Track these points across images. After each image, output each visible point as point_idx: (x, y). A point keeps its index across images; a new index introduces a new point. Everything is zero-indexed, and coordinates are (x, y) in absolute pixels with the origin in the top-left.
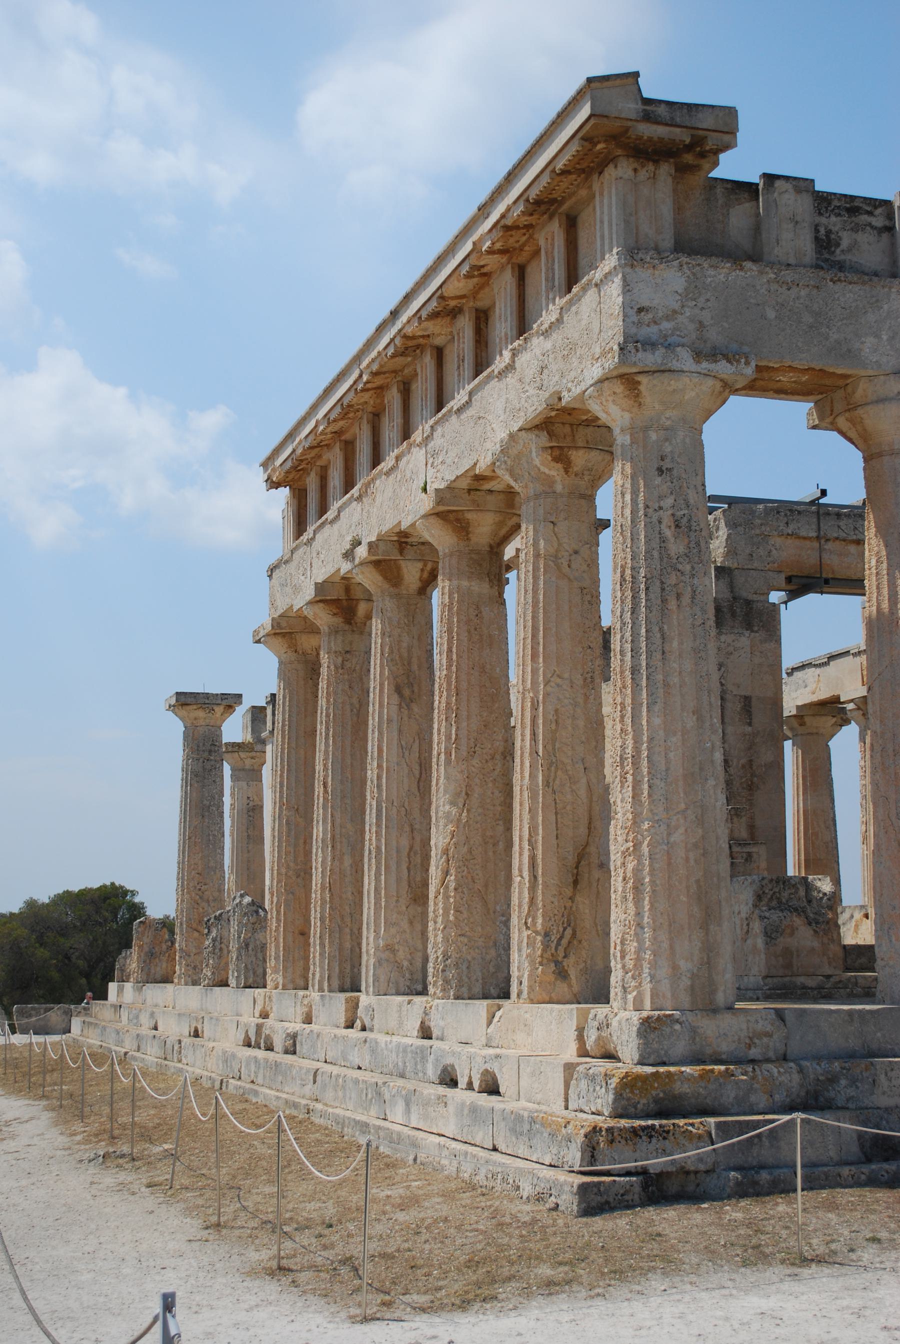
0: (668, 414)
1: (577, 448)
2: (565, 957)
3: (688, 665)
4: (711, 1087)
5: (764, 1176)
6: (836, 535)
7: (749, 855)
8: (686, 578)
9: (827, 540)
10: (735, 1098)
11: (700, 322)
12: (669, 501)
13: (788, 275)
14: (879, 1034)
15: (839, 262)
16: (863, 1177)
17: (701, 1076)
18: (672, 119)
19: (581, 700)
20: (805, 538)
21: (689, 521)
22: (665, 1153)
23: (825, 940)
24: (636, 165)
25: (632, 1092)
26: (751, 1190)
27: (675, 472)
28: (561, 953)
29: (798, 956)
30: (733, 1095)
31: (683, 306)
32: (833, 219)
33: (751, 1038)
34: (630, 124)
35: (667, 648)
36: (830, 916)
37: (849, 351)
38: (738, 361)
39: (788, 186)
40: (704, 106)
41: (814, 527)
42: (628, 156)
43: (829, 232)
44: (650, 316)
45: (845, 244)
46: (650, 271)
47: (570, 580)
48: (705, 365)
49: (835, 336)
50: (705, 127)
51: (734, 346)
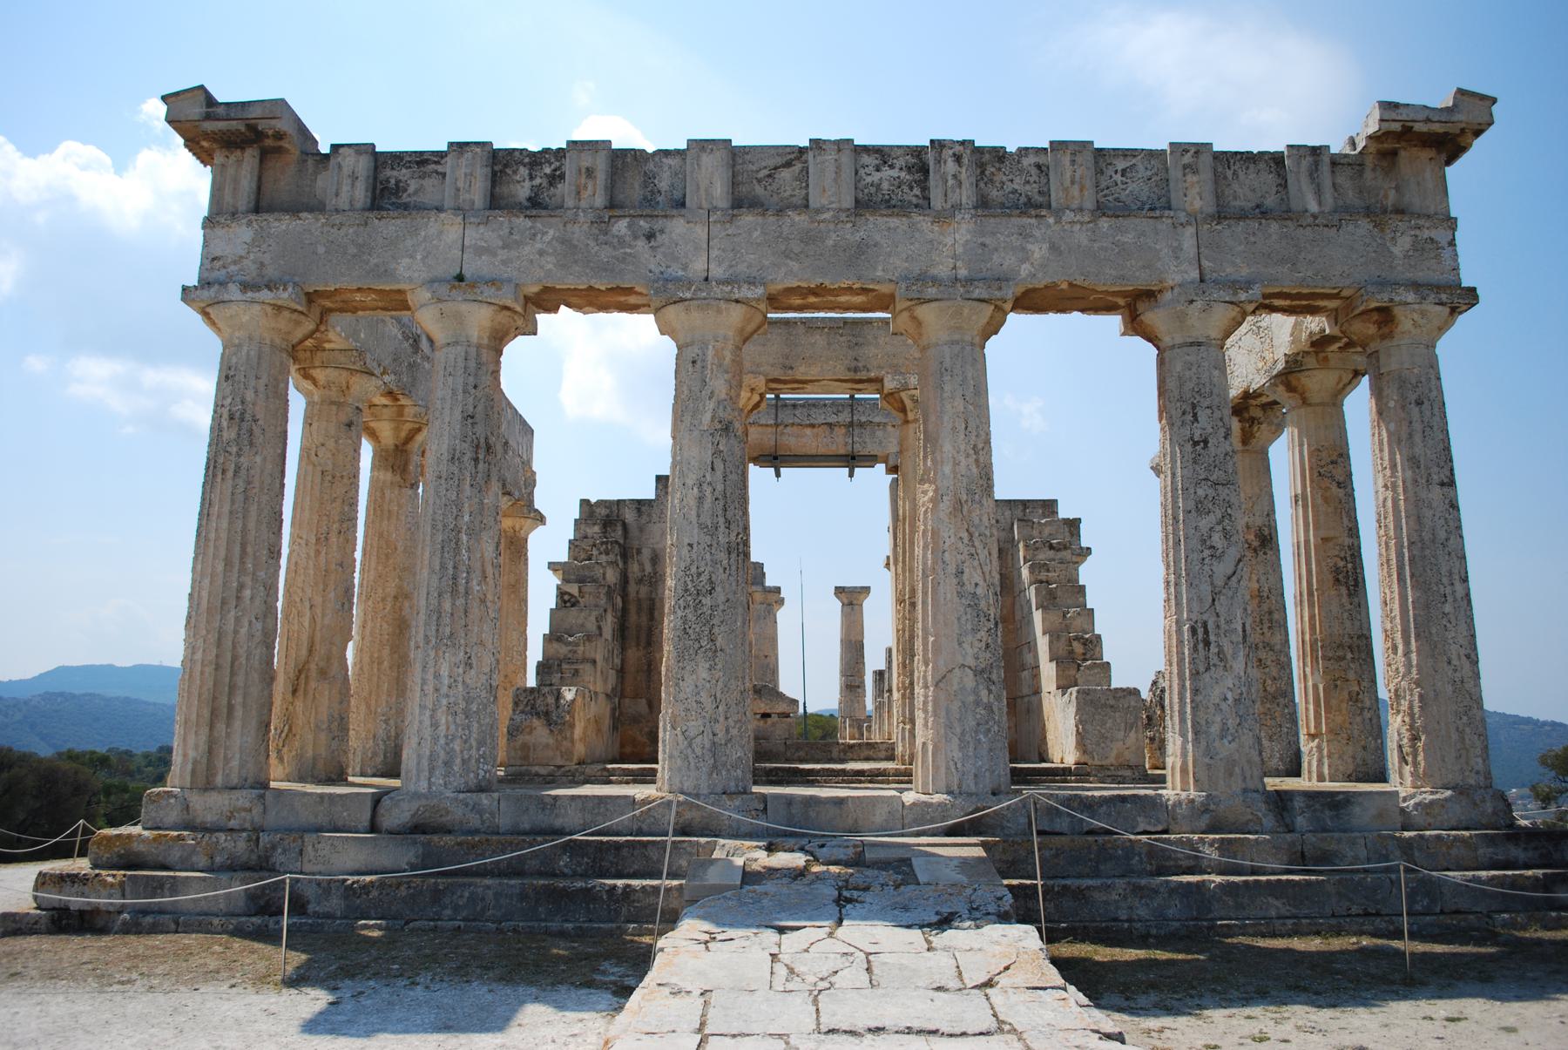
0: (237, 334)
1: (315, 367)
2: (283, 746)
3: (225, 524)
4: (161, 847)
5: (149, 919)
6: (791, 421)
7: (577, 671)
8: (232, 458)
9: (786, 426)
10: (181, 857)
11: (262, 264)
12: (229, 400)
13: (337, 219)
14: (345, 814)
15: (405, 204)
16: (231, 927)
17: (155, 839)
18: (227, 115)
19: (312, 554)
20: (767, 426)
21: (242, 414)
22: (83, 895)
23: (559, 738)
24: (227, 153)
25: (98, 848)
26: (134, 929)
27: (236, 378)
28: (281, 744)
29: (534, 750)
30: (178, 855)
31: (248, 253)
32: (404, 171)
33: (232, 813)
34: (197, 123)
35: (211, 512)
36: (568, 718)
37: (386, 271)
38: (277, 289)
39: (351, 151)
40: (249, 102)
41: (773, 416)
42: (222, 148)
43: (398, 182)
44: (221, 263)
45: (411, 190)
46: (226, 229)
47: (314, 465)
48: (250, 294)
49: (375, 261)
50: (254, 116)
51: (287, 278)
